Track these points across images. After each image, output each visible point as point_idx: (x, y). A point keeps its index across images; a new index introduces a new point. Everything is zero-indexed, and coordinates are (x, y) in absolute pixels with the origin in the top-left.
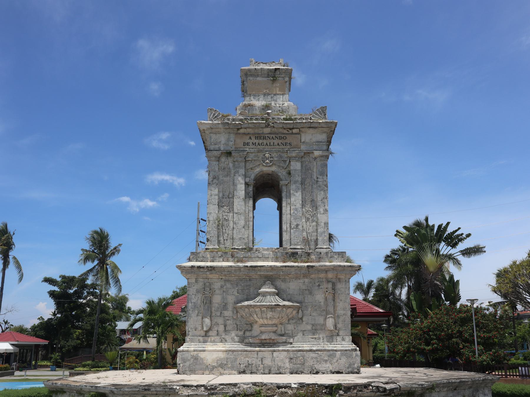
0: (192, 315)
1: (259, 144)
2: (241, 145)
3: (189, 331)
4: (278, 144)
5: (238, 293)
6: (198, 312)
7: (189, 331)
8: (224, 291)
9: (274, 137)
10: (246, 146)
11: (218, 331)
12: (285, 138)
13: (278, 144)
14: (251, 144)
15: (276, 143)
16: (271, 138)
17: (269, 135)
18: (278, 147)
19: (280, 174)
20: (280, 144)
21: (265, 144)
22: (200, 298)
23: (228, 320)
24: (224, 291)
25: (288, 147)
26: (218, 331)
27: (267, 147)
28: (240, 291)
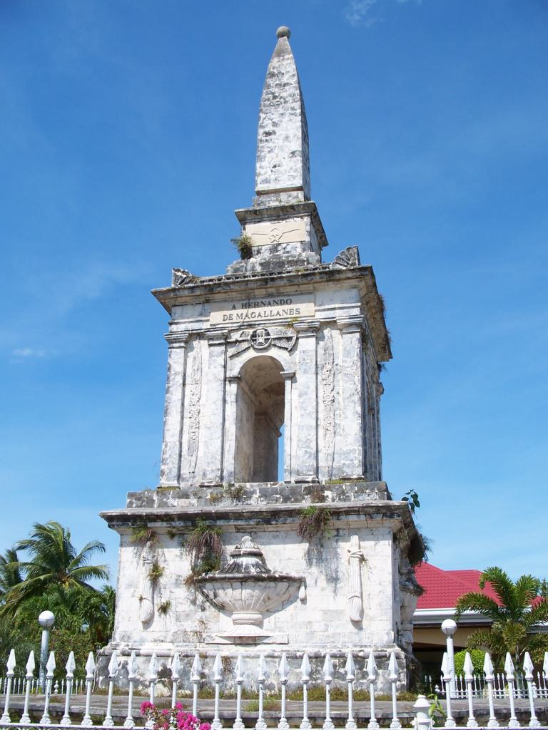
1: (247, 316)
4: (278, 313)
9: (272, 302)
13: (278, 313)
14: (235, 317)
15: (275, 312)
16: (267, 303)
17: (264, 300)
20: (281, 313)
25: (294, 316)
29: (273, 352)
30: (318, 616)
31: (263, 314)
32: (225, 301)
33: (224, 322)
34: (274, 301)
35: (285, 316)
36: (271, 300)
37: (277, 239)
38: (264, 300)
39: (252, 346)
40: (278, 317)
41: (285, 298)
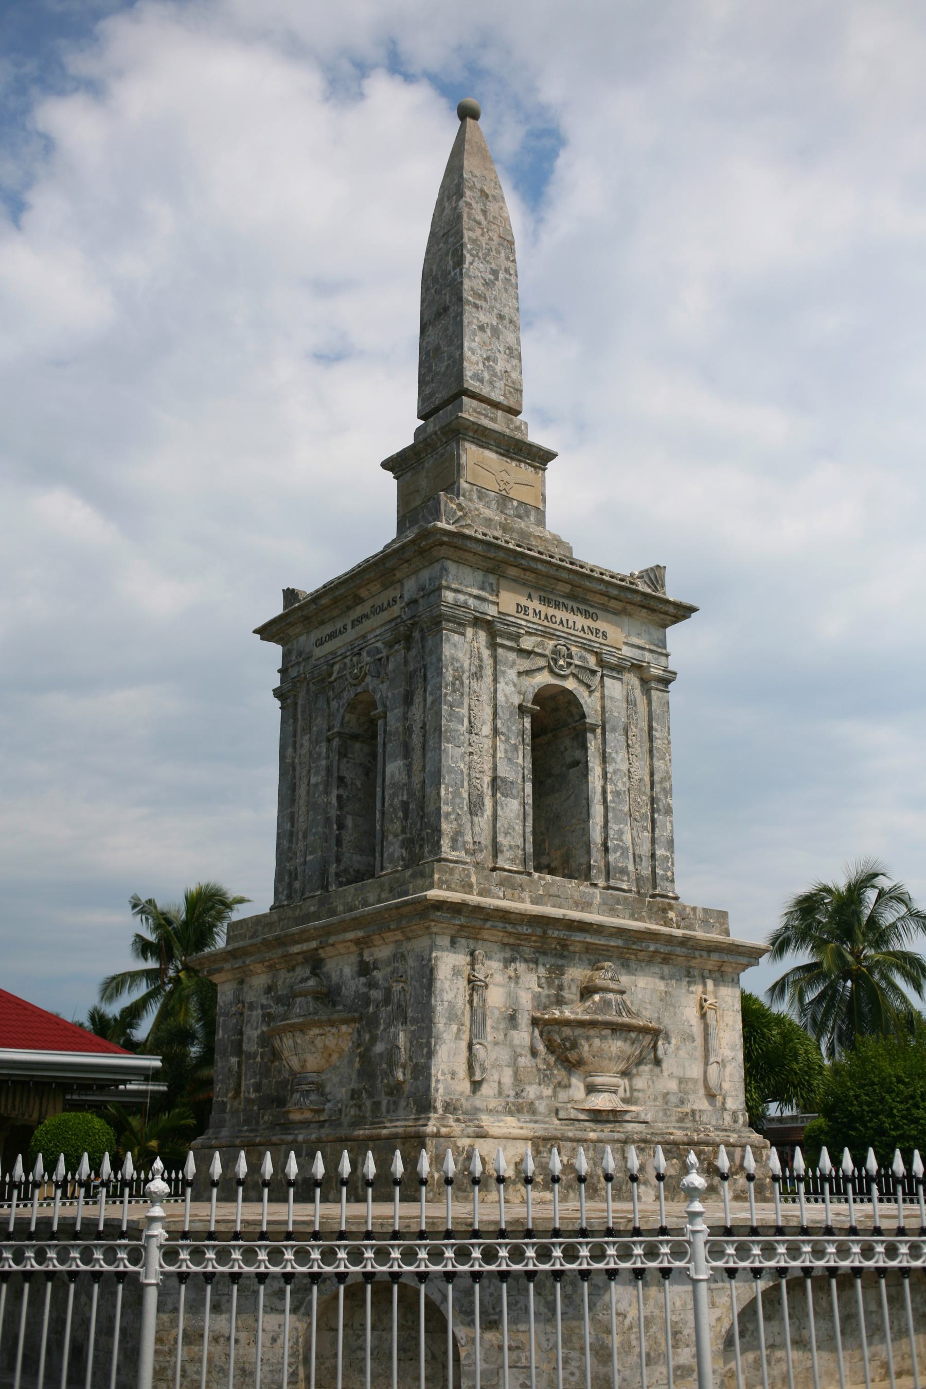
0: (445, 1036)
2: (512, 610)
3: (438, 1081)
4: (583, 629)
5: (540, 986)
6: (459, 1030)
7: (438, 1081)
8: (510, 978)
9: (575, 609)
10: (521, 615)
11: (499, 1083)
12: (594, 616)
18: (582, 634)
19: (582, 701)
21: (558, 621)
22: (462, 990)
23: (521, 1055)
24: (510, 978)
25: (601, 640)
26: (499, 1083)
27: (560, 628)
28: (543, 980)
29: (570, 684)
30: (673, 1086)
31: (571, 624)
32: (514, 580)
33: (517, 615)
34: (578, 609)
35: (590, 637)
36: (575, 606)
37: (508, 487)
38: (566, 602)
39: (549, 666)
40: (582, 634)
41: (591, 610)
